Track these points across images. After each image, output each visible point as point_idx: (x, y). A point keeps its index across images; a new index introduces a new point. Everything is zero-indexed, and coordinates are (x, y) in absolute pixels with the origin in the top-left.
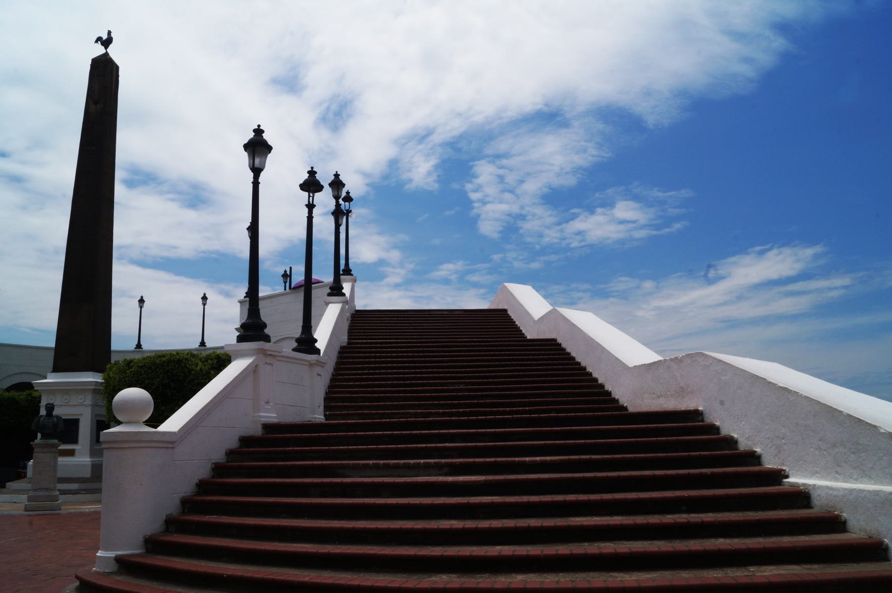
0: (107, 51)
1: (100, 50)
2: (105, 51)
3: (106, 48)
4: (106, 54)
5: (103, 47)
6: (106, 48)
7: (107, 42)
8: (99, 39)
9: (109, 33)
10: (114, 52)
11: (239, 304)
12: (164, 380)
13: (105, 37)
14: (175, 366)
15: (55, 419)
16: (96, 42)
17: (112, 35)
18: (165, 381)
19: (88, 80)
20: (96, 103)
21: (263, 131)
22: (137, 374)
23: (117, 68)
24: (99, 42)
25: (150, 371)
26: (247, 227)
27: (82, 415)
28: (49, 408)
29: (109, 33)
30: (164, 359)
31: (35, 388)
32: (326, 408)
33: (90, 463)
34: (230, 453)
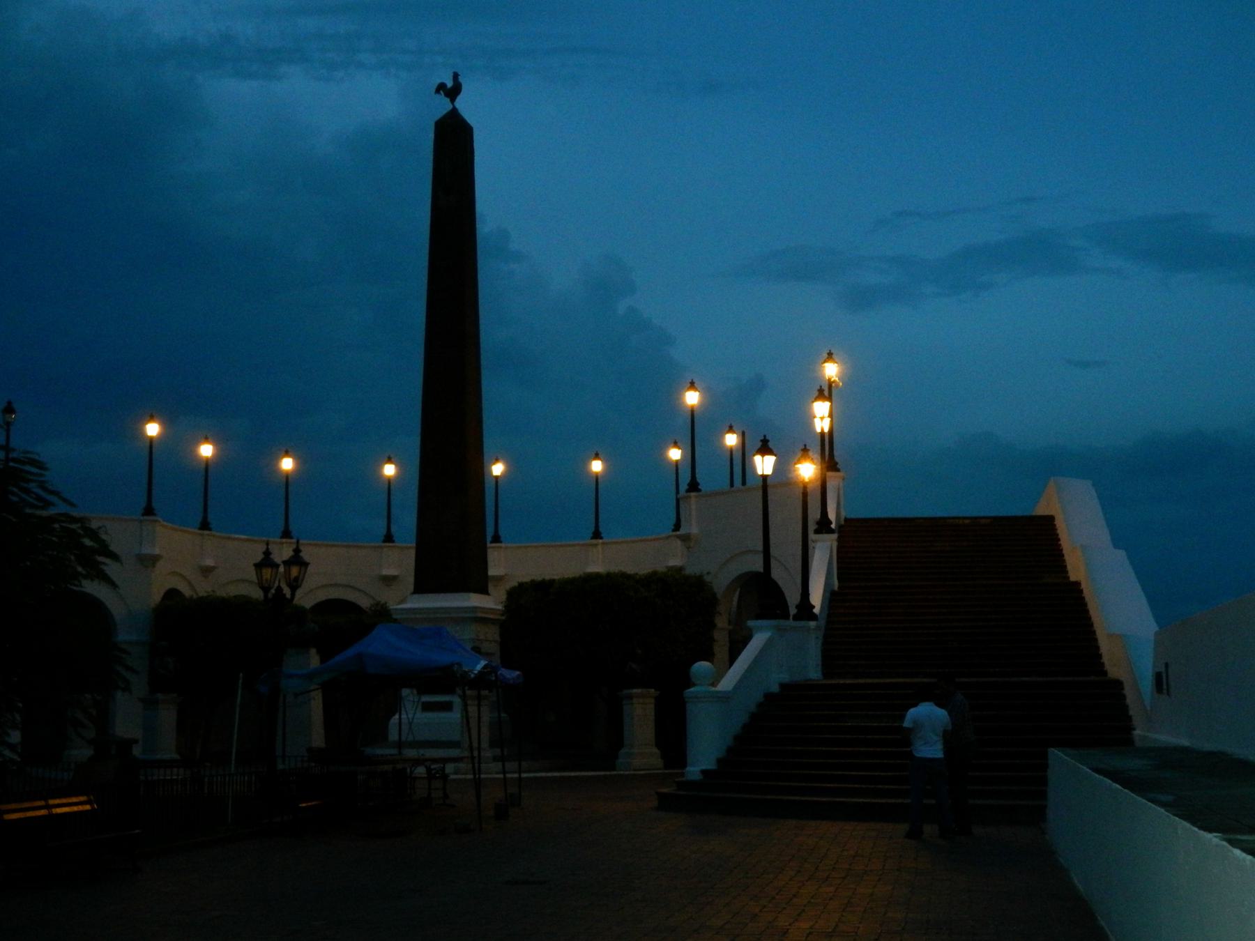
1: (442, 106)
2: (450, 107)
4: (454, 115)
5: (448, 100)
6: (453, 100)
8: (441, 88)
9: (456, 76)
10: (464, 104)
13: (450, 84)
16: (438, 91)
17: (461, 79)
21: (768, 441)
24: (442, 92)
29: (456, 76)
31: (395, 617)
34: (760, 705)
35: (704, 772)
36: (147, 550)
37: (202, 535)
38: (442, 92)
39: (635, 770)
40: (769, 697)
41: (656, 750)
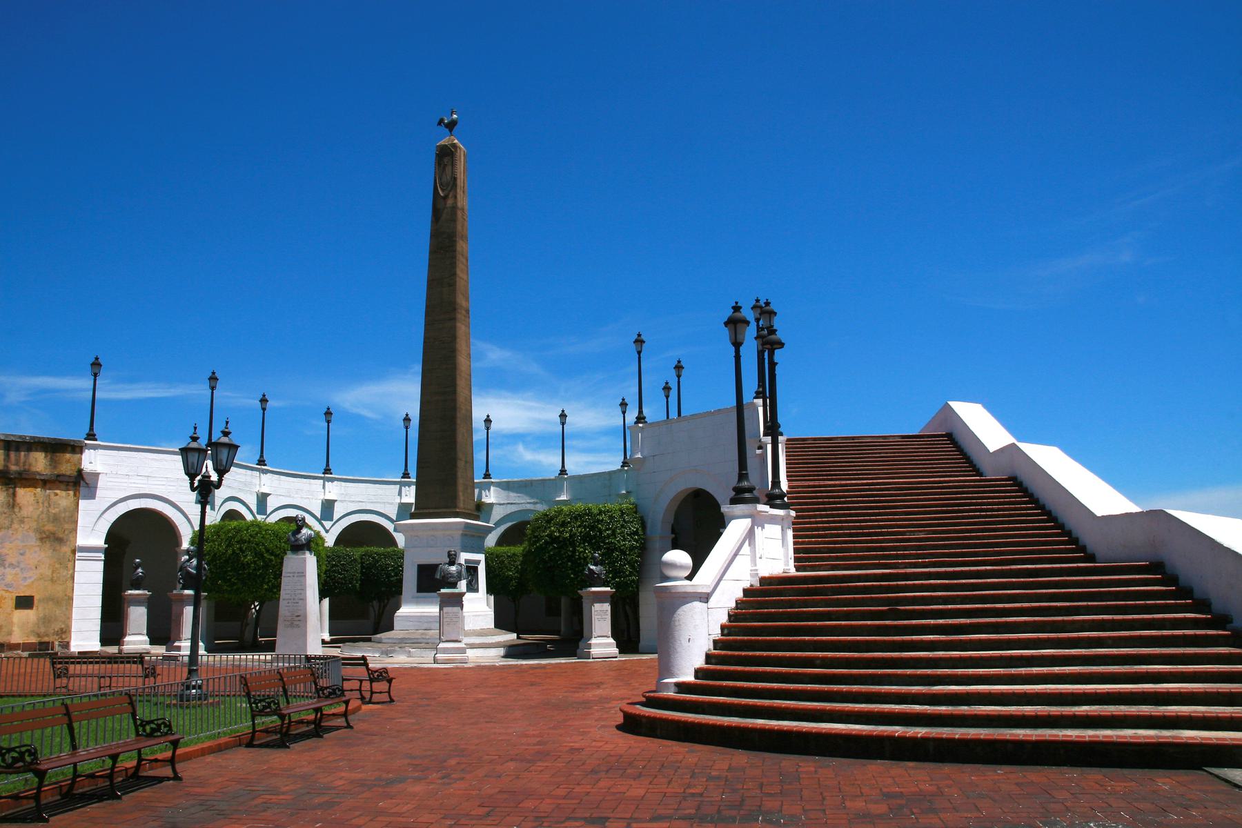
32: (796, 560)
35: (682, 687)
39: (593, 658)
40: (746, 592)
41: (611, 640)
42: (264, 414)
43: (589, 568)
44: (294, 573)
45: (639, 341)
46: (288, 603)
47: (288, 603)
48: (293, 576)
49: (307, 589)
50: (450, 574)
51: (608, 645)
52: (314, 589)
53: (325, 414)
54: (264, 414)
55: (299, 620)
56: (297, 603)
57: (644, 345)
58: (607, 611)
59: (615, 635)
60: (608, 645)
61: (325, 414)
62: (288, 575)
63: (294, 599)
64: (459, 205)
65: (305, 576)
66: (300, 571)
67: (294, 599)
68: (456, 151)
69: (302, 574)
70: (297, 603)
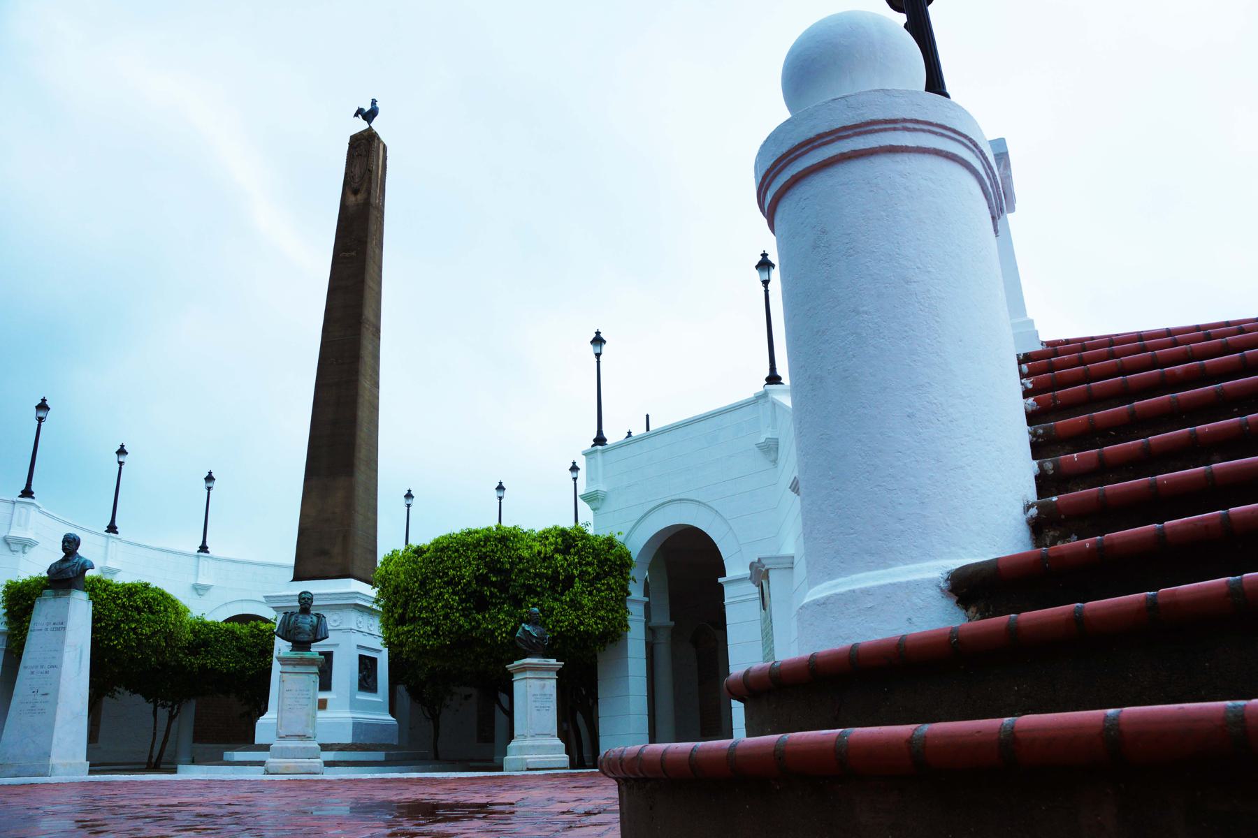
0: (370, 127)
1: (361, 125)
2: (367, 126)
3: (369, 122)
5: (366, 122)
6: (369, 122)
7: (369, 115)
8: (359, 112)
9: (374, 102)
11: (584, 457)
12: (479, 570)
13: (367, 108)
14: (496, 546)
15: (315, 619)
16: (356, 115)
17: (378, 104)
18: (481, 571)
19: (345, 166)
20: (356, 192)
22: (434, 561)
23: (385, 146)
24: (359, 115)
25: (456, 554)
26: (591, 339)
27: (336, 645)
28: (304, 599)
29: (374, 102)
30: (477, 536)
33: (351, 721)
36: (16, 533)
37: (107, 537)
38: (359, 115)
39: (529, 769)
41: (558, 742)
42: (120, 469)
43: (523, 628)
44: (48, 624)
45: (598, 340)
46: (32, 673)
47: (32, 673)
48: (47, 629)
49: (66, 649)
50: (299, 628)
51: (553, 749)
52: (81, 652)
53: (205, 479)
54: (120, 469)
55: (47, 702)
56: (46, 672)
57: (604, 347)
58: (552, 695)
59: (562, 735)
60: (553, 749)
61: (205, 479)
62: (39, 627)
63: (42, 667)
64: (375, 201)
65: (65, 628)
66: (56, 621)
67: (42, 667)
68: (373, 140)
69: (61, 627)
70: (46, 672)
